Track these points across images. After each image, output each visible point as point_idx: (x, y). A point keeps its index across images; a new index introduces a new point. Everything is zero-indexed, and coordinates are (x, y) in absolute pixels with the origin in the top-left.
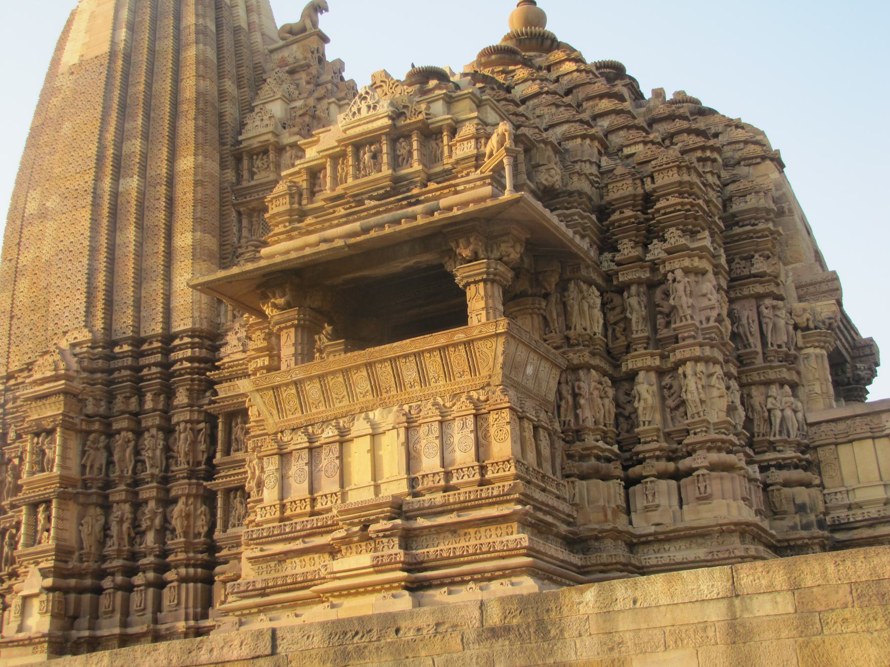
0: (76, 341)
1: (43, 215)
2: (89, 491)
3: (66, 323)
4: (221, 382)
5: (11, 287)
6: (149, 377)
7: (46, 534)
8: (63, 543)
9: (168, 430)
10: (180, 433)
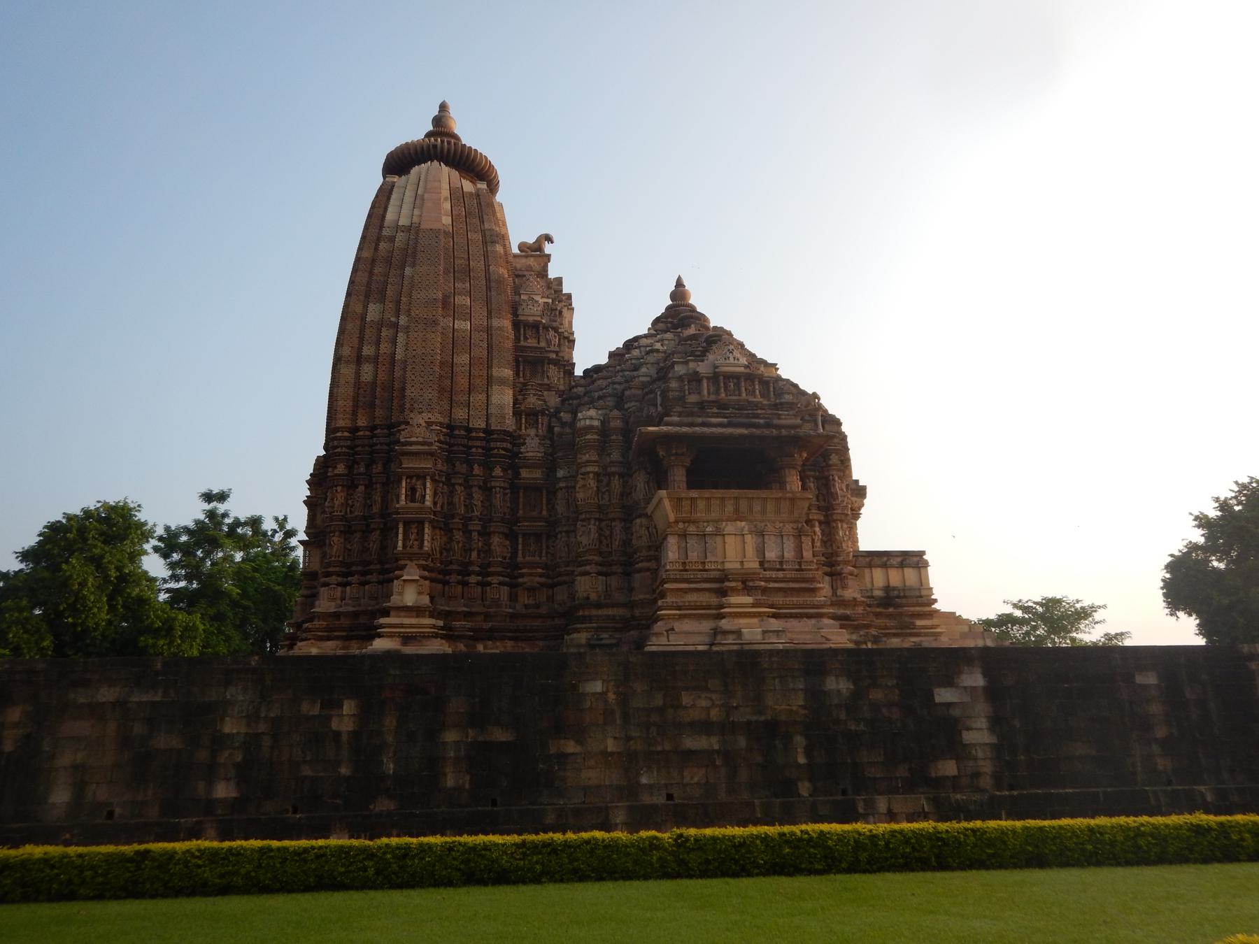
9: (487, 490)
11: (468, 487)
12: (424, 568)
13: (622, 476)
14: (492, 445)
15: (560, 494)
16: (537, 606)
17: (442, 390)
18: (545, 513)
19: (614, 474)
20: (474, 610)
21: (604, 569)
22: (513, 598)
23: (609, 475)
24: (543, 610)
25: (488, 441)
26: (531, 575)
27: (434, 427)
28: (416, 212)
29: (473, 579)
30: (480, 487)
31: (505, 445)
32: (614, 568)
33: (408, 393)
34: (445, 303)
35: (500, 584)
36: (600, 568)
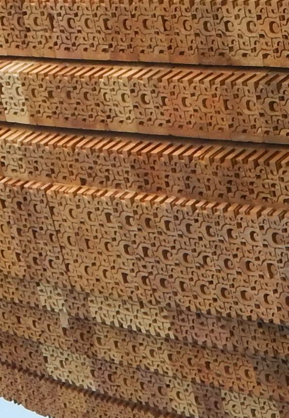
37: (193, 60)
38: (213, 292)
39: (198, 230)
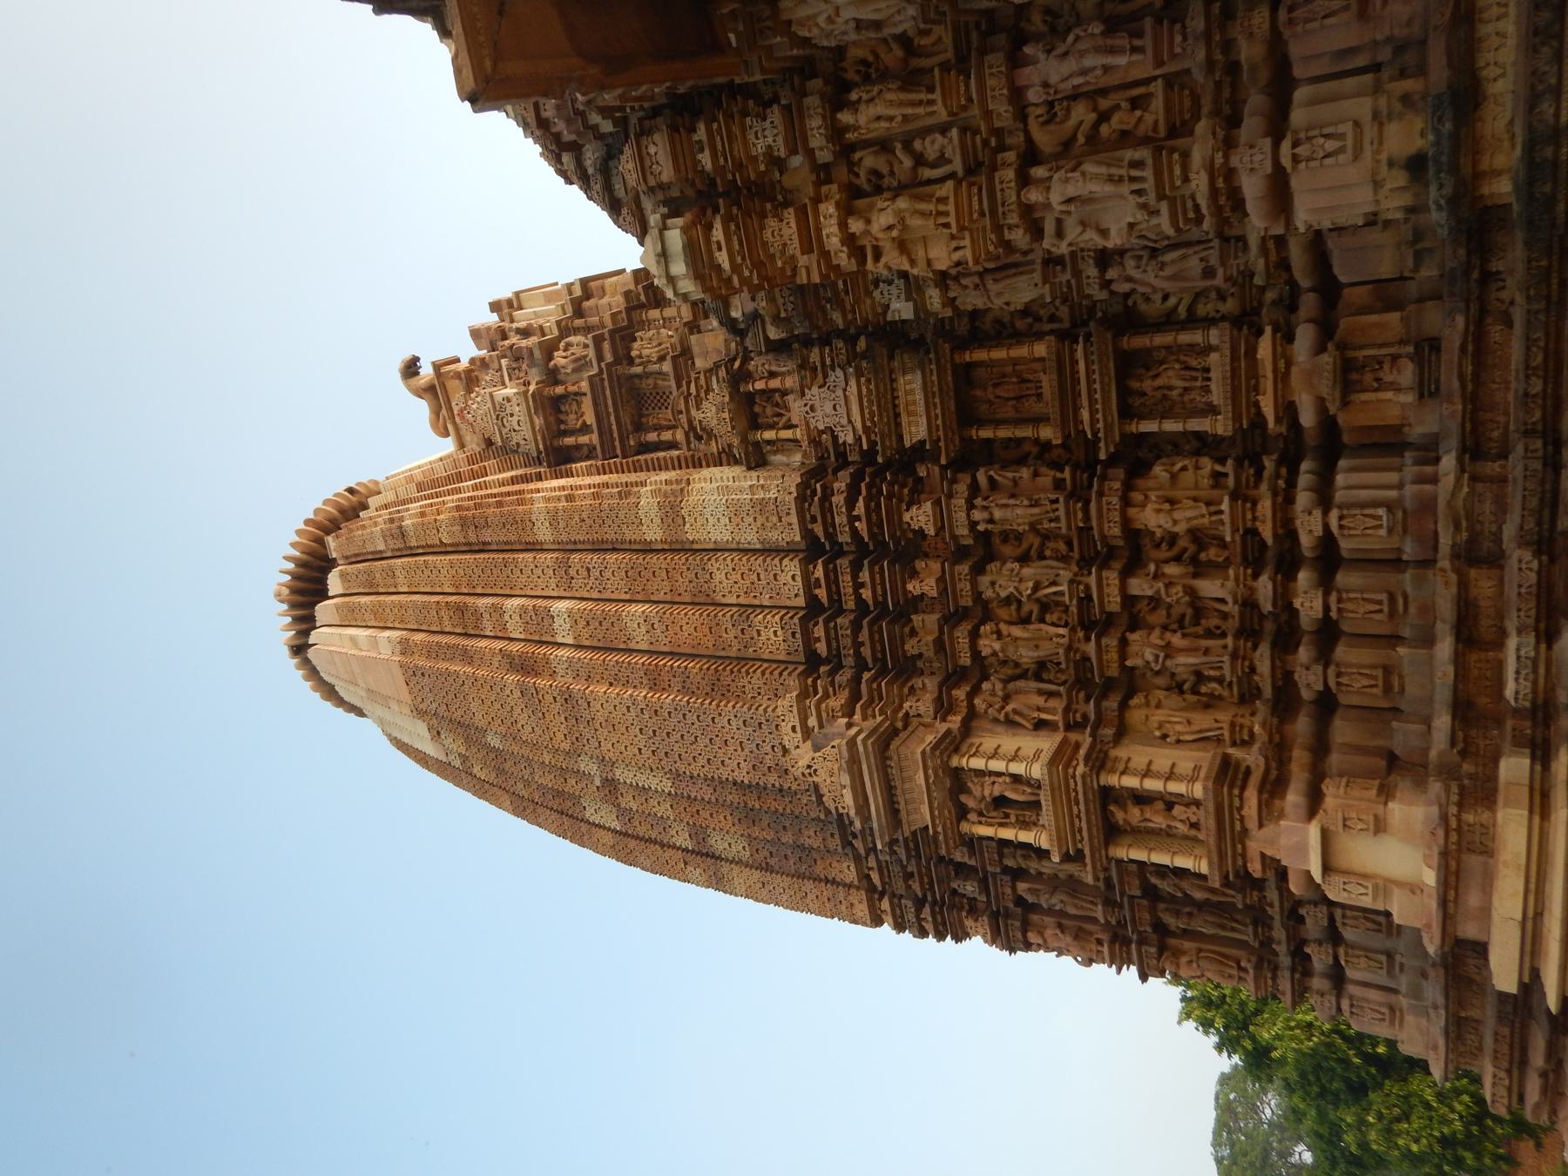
0: (798, 729)
1: (611, 787)
2: (1092, 717)
3: (769, 749)
4: (900, 438)
5: (725, 868)
6: (879, 591)
7: (1178, 810)
8: (1202, 774)
9: (984, 550)
10: (991, 521)
11: (983, 611)
12: (1274, 787)
13: (838, 99)
14: (844, 538)
15: (972, 300)
16: (1427, 349)
17: (717, 690)
18: (1040, 349)
19: (836, 133)
20: (1445, 605)
21: (1256, 102)
22: (1386, 444)
23: (846, 150)
24: (1453, 329)
25: (840, 551)
26: (1282, 379)
27: (812, 722)
28: (395, 706)
29: (1309, 604)
30: (978, 569)
31: (838, 500)
32: (1249, 51)
33: (742, 776)
34: (526, 666)
35: (1324, 498)
36: (1251, 125)
37: (688, 600)
38: (702, 761)
39: (692, 718)
